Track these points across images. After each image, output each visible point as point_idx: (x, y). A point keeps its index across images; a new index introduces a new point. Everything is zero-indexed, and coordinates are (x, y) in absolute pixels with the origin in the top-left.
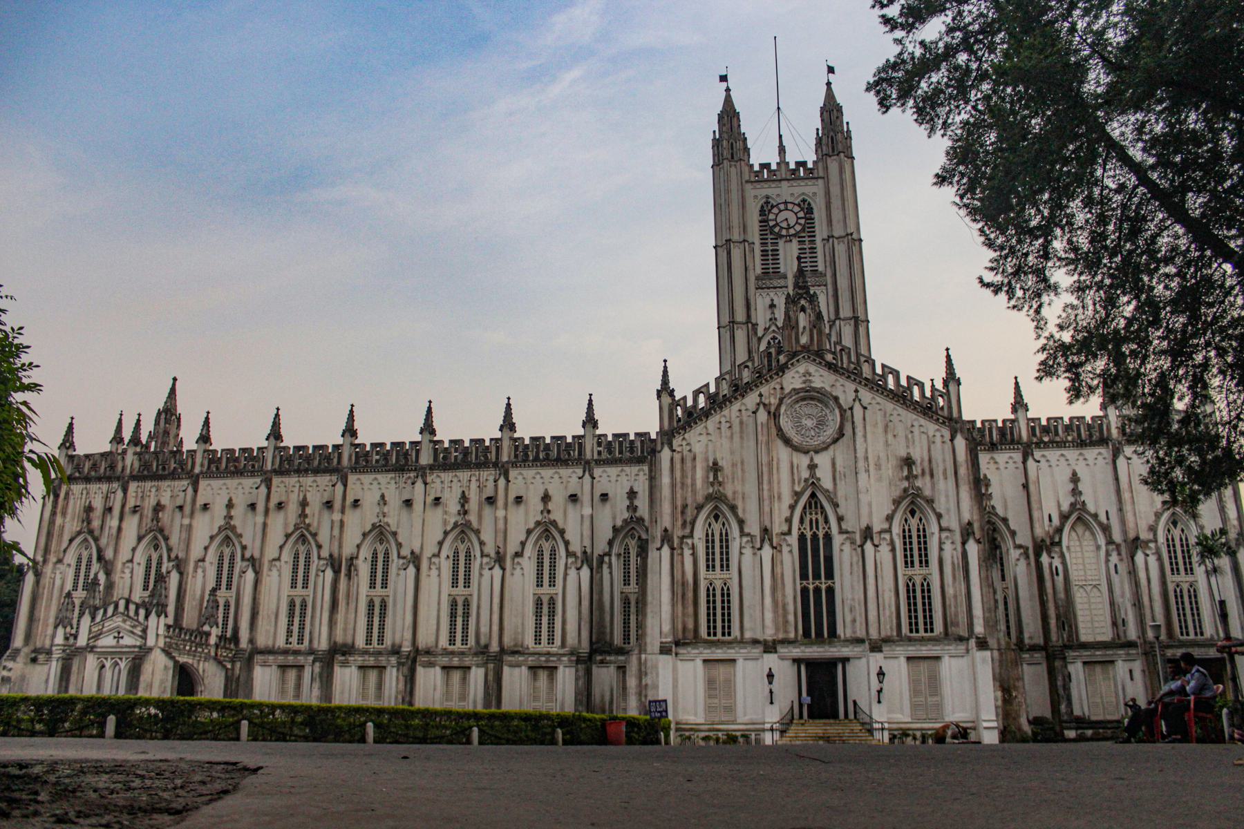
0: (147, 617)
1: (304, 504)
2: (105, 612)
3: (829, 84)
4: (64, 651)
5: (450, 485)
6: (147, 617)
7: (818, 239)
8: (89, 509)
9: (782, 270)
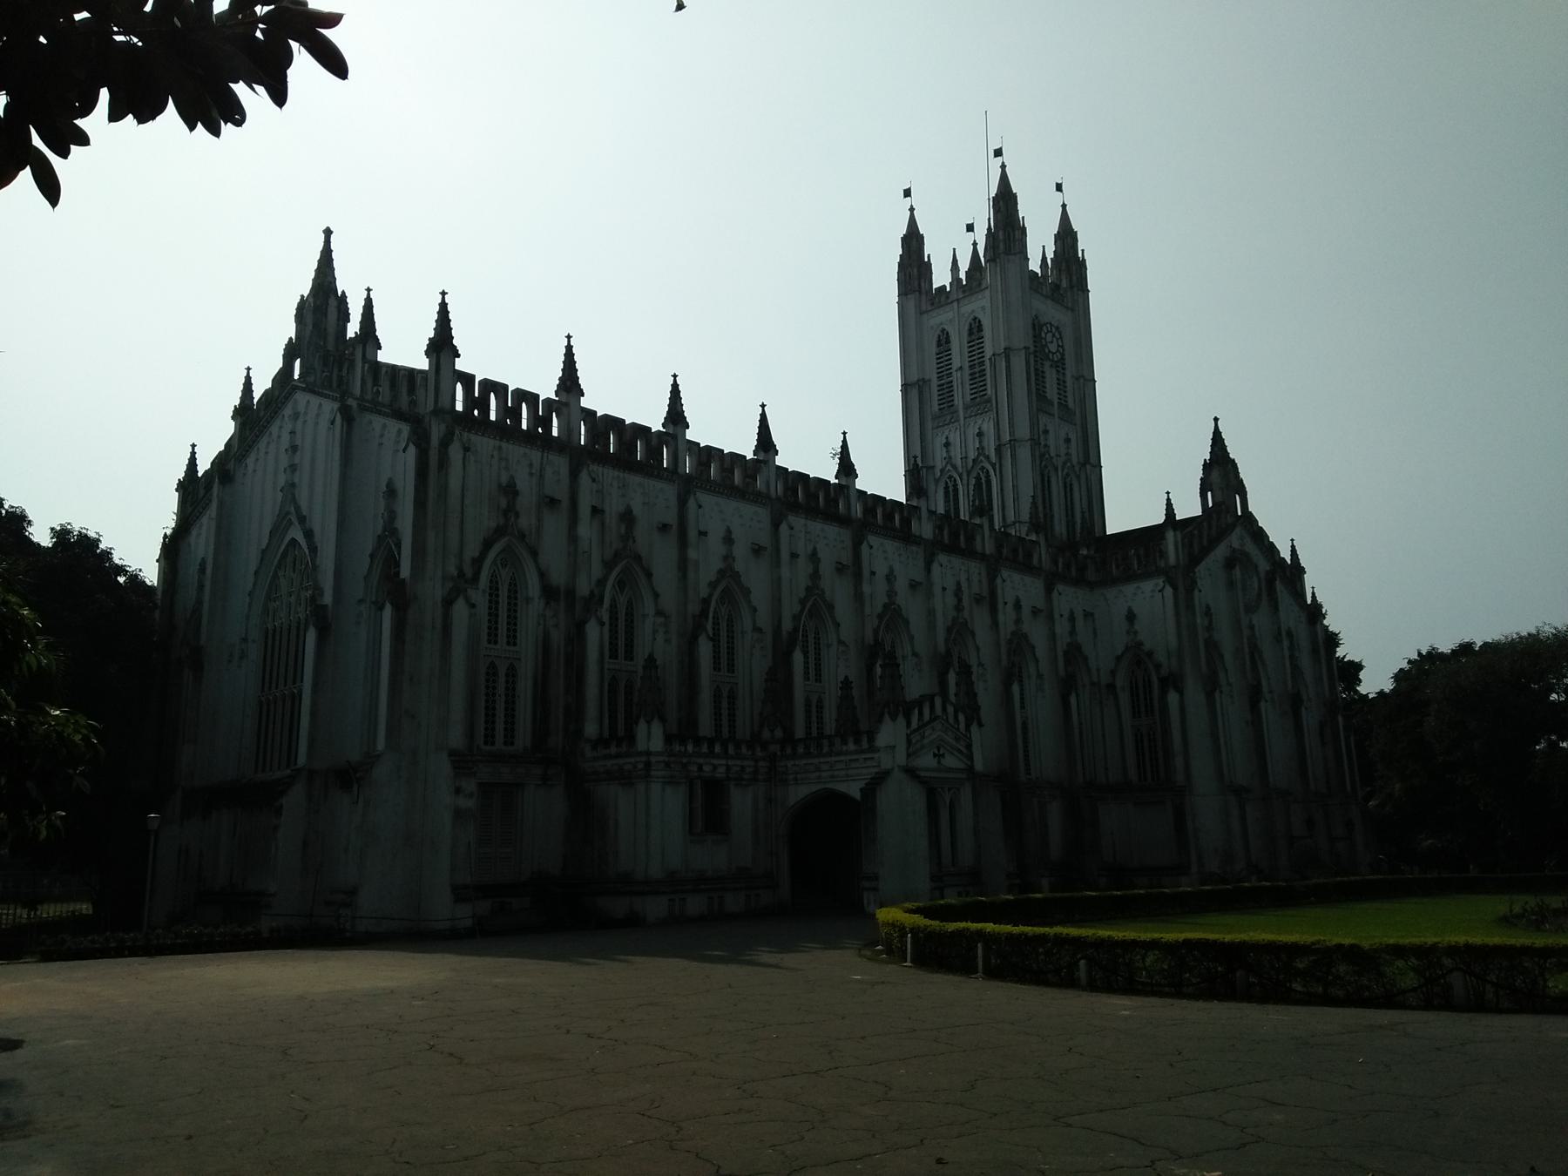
0: (968, 727)
1: (814, 557)
2: (921, 714)
4: (667, 764)
5: (948, 570)
6: (968, 727)
8: (510, 490)
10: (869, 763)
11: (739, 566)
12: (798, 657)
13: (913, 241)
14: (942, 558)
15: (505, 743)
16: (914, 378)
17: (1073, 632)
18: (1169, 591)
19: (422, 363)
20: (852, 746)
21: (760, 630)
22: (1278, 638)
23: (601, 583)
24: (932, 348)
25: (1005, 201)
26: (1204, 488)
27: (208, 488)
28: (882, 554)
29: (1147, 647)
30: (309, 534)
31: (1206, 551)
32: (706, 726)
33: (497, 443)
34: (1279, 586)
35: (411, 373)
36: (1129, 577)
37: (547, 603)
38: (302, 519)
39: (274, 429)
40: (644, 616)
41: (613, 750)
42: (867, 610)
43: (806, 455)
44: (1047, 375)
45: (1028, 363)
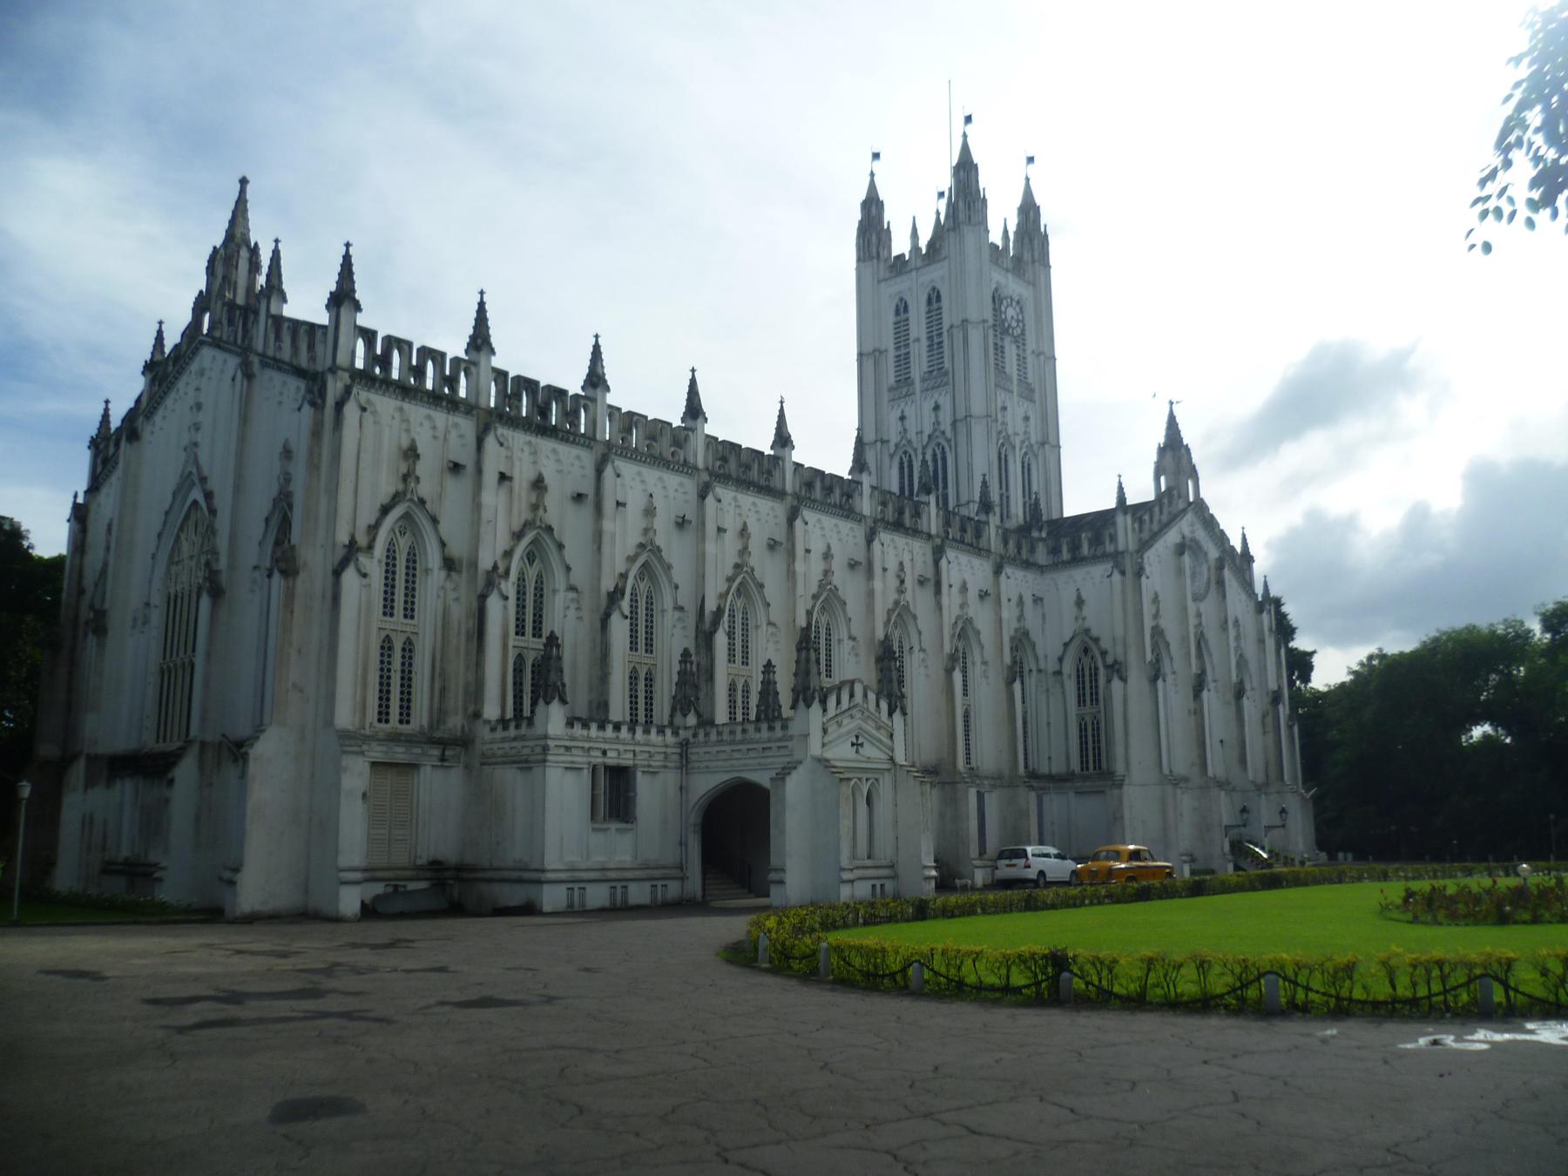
1: (744, 532)
3: (1027, 179)
5: (894, 549)
6: (890, 714)
7: (1029, 349)
9: (1007, 370)
10: (783, 752)
11: (660, 541)
12: (721, 639)
13: (872, 207)
14: (884, 536)
15: (401, 722)
16: (868, 348)
17: (1021, 618)
18: (1117, 576)
19: (322, 318)
20: (765, 734)
21: (681, 609)
22: (1224, 626)
23: (508, 554)
24: (891, 318)
25: (965, 169)
26: (1159, 471)
27: (117, 445)
28: (821, 531)
29: (1094, 633)
30: (209, 496)
31: (1155, 536)
32: (618, 708)
33: (399, 403)
34: (1227, 573)
35: (312, 327)
36: (1077, 560)
37: (449, 576)
38: (203, 480)
39: (181, 385)
40: (554, 591)
41: (512, 732)
42: (800, 590)
43: (740, 423)
44: (1007, 350)
45: (985, 337)
